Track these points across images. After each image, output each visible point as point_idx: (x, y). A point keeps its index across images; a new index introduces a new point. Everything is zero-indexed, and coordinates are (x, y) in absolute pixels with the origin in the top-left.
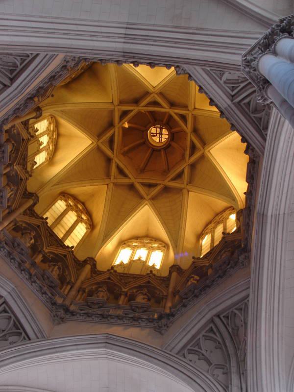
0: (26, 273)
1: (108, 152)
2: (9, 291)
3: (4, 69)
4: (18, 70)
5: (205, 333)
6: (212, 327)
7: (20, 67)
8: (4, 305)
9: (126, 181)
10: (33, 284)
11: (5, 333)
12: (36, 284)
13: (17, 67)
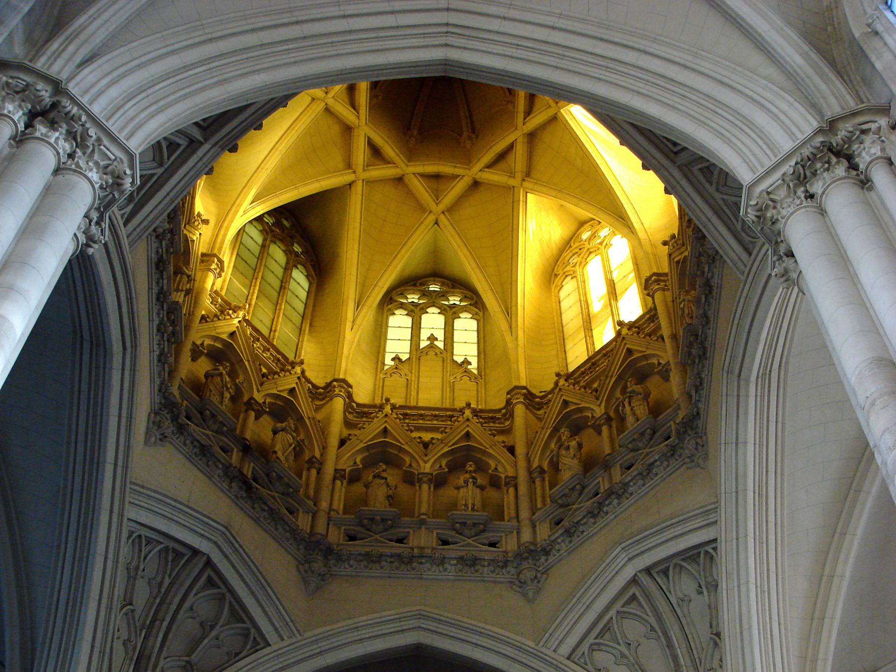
0: (607, 502)
1: (459, 187)
2: (626, 559)
3: (172, 570)
5: (711, 184)
6: (700, 169)
8: (653, 572)
9: (520, 150)
10: (631, 490)
11: (703, 584)
12: (631, 484)
13: (166, 549)
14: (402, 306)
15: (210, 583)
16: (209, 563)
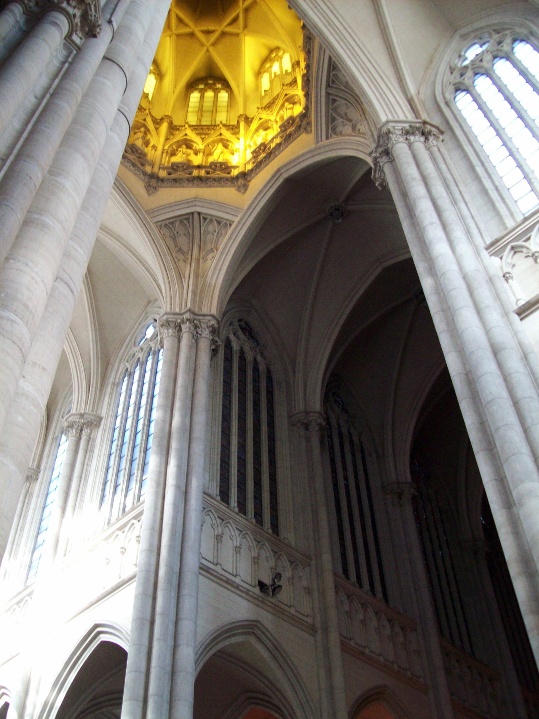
4: (182, 218)
7: (179, 218)
14: (264, 72)
15: (205, 219)
16: (199, 214)
